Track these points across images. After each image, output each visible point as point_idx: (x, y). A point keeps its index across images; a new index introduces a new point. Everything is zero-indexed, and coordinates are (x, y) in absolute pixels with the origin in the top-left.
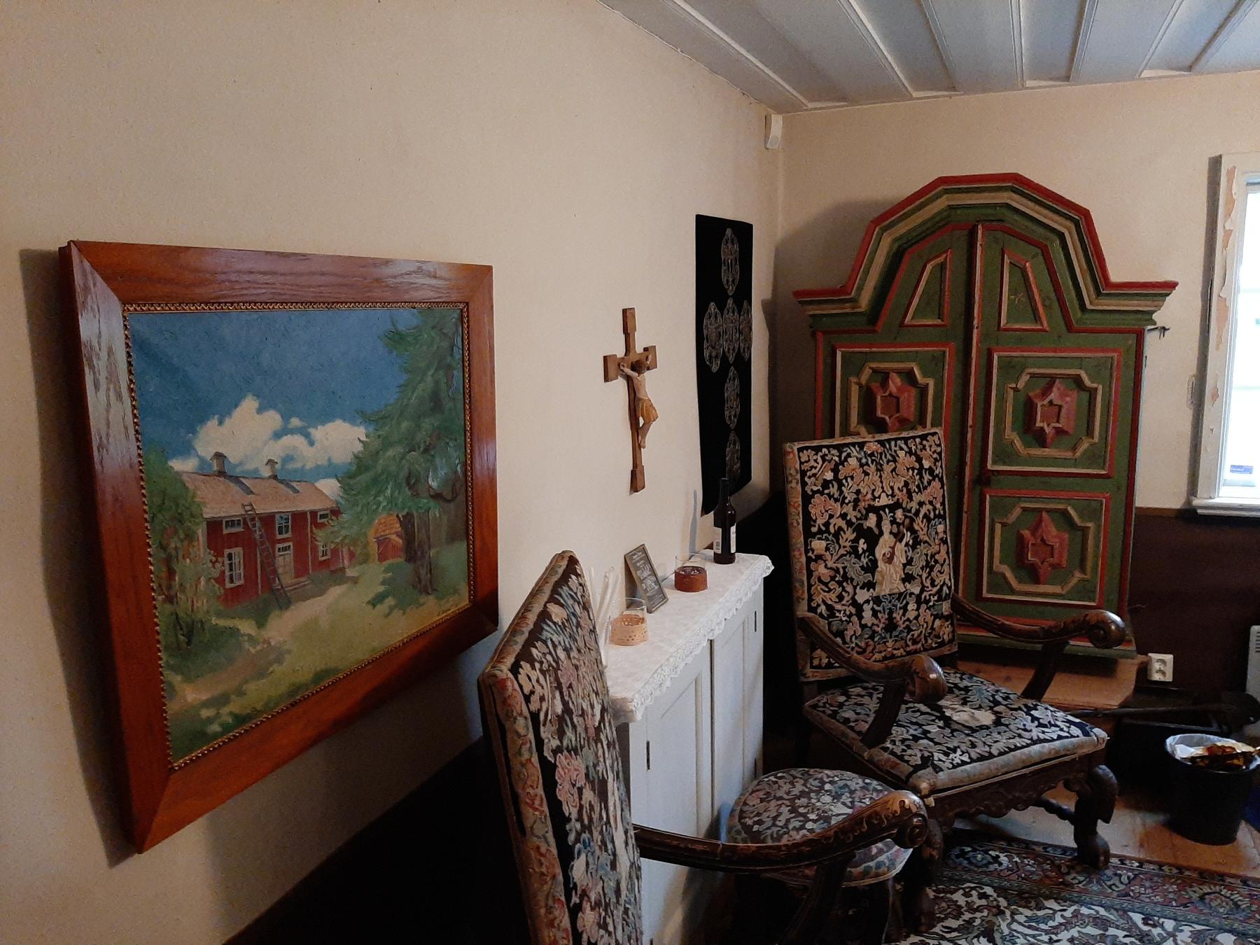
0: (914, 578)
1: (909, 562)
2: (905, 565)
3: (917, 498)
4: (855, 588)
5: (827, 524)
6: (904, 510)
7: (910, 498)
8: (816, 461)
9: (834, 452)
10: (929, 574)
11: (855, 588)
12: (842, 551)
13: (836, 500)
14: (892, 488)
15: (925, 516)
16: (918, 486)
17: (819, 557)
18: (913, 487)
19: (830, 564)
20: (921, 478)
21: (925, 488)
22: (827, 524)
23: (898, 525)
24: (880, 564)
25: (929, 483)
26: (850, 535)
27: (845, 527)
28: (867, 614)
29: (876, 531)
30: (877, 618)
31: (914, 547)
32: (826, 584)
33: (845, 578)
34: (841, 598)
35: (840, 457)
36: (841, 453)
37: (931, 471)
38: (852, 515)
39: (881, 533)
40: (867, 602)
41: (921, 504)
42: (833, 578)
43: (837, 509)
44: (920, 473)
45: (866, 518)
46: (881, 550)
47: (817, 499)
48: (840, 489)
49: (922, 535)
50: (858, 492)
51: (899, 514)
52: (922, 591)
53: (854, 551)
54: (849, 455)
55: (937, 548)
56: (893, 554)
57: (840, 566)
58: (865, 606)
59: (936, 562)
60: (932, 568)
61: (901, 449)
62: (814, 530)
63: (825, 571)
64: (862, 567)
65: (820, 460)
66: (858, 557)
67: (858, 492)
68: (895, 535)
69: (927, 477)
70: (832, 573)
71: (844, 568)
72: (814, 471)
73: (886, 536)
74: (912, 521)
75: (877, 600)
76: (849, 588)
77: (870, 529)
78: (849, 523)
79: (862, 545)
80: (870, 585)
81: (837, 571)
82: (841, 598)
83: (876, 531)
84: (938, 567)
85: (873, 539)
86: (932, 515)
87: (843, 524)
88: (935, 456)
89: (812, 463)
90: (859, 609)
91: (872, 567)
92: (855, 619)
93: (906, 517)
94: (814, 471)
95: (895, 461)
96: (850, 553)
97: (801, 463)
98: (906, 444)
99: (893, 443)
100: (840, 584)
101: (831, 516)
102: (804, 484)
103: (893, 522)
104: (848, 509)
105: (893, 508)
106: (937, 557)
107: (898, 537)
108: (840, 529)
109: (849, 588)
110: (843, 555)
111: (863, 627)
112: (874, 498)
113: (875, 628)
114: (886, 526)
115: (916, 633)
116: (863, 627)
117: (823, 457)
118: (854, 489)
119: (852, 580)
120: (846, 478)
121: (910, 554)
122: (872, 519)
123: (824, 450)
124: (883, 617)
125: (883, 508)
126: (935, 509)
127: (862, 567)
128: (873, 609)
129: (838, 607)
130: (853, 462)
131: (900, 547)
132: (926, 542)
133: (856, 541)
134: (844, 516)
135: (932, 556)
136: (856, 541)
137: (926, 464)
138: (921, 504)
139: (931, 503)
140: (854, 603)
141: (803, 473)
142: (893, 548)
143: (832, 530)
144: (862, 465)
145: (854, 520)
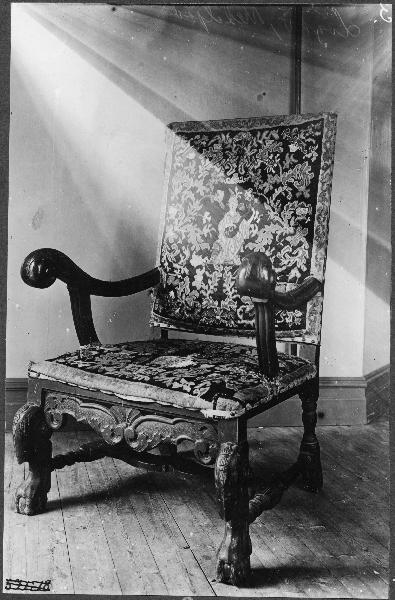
1: (252, 240)
2: (246, 241)
3: (272, 180)
4: (191, 253)
6: (254, 190)
7: (264, 178)
10: (275, 253)
11: (191, 253)
14: (246, 169)
15: (280, 196)
16: (277, 169)
17: (172, 221)
19: (176, 229)
20: (282, 158)
21: (286, 170)
23: (246, 202)
24: (221, 236)
25: (292, 166)
26: (197, 206)
27: (193, 198)
28: (199, 278)
29: (222, 206)
30: (206, 283)
31: (261, 226)
32: (170, 245)
35: (208, 142)
36: (210, 139)
37: (298, 155)
38: (201, 189)
39: (227, 209)
40: (200, 267)
41: (276, 186)
42: (176, 241)
44: (282, 158)
45: (215, 192)
46: (227, 222)
47: (179, 173)
54: (217, 142)
57: (183, 231)
58: (198, 271)
60: (279, 249)
61: (272, 138)
64: (203, 236)
71: (187, 234)
72: (181, 151)
73: (232, 212)
77: (217, 203)
78: (198, 196)
79: (207, 217)
80: (205, 253)
82: (178, 259)
83: (222, 206)
84: (288, 249)
85: (218, 213)
87: (192, 196)
88: (309, 140)
90: (192, 271)
92: (187, 279)
94: (181, 151)
96: (194, 222)
98: (279, 134)
99: (264, 134)
103: (241, 200)
104: (199, 185)
106: (288, 239)
107: (246, 214)
109: (187, 253)
111: (192, 288)
113: (204, 293)
114: (233, 202)
115: (248, 309)
119: (191, 245)
121: (255, 232)
122: (221, 194)
123: (198, 137)
124: (213, 284)
126: (295, 191)
127: (203, 236)
128: (204, 275)
129: (175, 265)
131: (247, 224)
132: (277, 222)
133: (202, 212)
134: (194, 189)
135: (281, 237)
136: (202, 212)
137: (293, 148)
139: (290, 185)
140: (189, 265)
142: (238, 224)
144: (224, 151)
145: (202, 194)
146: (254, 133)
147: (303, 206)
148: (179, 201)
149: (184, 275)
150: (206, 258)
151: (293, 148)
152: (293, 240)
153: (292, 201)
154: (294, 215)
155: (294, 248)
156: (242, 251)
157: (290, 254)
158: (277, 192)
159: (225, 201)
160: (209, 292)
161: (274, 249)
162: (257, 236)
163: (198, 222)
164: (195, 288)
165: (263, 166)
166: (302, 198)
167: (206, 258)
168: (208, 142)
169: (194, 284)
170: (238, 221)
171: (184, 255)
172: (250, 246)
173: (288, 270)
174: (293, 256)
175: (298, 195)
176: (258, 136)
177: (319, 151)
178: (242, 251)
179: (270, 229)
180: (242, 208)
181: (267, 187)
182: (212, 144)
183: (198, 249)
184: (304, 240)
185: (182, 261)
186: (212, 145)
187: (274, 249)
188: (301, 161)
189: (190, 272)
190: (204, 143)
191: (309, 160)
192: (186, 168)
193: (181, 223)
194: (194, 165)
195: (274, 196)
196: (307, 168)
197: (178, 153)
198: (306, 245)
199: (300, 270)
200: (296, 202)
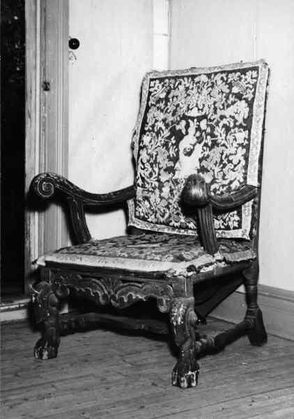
0: (208, 171)
2: (201, 160)
3: (220, 113)
4: (160, 169)
5: (153, 126)
7: (215, 112)
8: (158, 87)
9: (172, 81)
12: (159, 144)
13: (162, 111)
17: (145, 146)
18: (219, 105)
19: (149, 151)
20: (227, 98)
22: (153, 126)
25: (233, 103)
26: (166, 133)
27: (164, 128)
28: (166, 190)
31: (211, 148)
33: (155, 161)
34: (151, 174)
36: (176, 81)
39: (187, 133)
40: (168, 181)
41: (222, 117)
42: (148, 161)
43: (161, 116)
48: (166, 105)
49: (220, 140)
50: (178, 106)
51: (203, 124)
52: (214, 181)
53: (166, 145)
54: (180, 84)
55: (233, 150)
56: (192, 151)
59: (230, 162)
60: (225, 165)
62: (146, 129)
63: (146, 155)
65: (161, 86)
66: (168, 149)
67: (178, 106)
68: (197, 138)
69: (232, 99)
70: (148, 157)
74: (213, 128)
75: (176, 182)
76: (156, 170)
78: (167, 126)
80: (171, 170)
81: (151, 156)
83: (184, 132)
84: (230, 166)
85: (179, 136)
86: (232, 125)
89: (156, 88)
91: (176, 159)
92: (157, 191)
93: (208, 125)
95: (212, 87)
96: (163, 145)
97: (150, 87)
100: (152, 165)
101: (156, 121)
102: (148, 100)
103: (198, 129)
105: (200, 119)
106: (230, 158)
108: (160, 128)
109: (156, 170)
110: (159, 146)
111: (161, 198)
112: (188, 109)
113: (170, 201)
114: (192, 130)
116: (161, 198)
117: (163, 86)
118: (178, 102)
119: (159, 163)
120: (173, 98)
121: (206, 153)
125: (192, 119)
126: (236, 121)
127: (169, 157)
130: (181, 88)
131: (199, 147)
133: (169, 138)
138: (222, 117)
140: (159, 181)
141: (150, 93)
143: (156, 130)
146: (209, 76)
147: (240, 132)
148: (153, 131)
149: (154, 188)
150: (172, 174)
151: (235, 90)
152: (235, 159)
153: (234, 128)
154: (235, 139)
155: (235, 166)
156: (199, 168)
157: (233, 170)
158: (225, 121)
159: (187, 126)
160: (175, 200)
161: (222, 165)
162: (208, 156)
163: (166, 145)
164: (164, 198)
165: (215, 103)
166: (241, 126)
167: (172, 174)
168: (174, 85)
169: (162, 195)
170: (193, 143)
171: (154, 171)
172: (204, 163)
173: (231, 182)
174: (234, 171)
175: (238, 124)
176: (212, 77)
177: (254, 93)
178: (199, 168)
179: (217, 150)
180: (198, 134)
181: (217, 117)
182: (177, 87)
183: (165, 167)
184: (242, 159)
185: (154, 176)
186: (177, 87)
187: (222, 165)
188: (241, 100)
189: (159, 186)
190: (172, 86)
191: (246, 100)
192: (158, 105)
193: (154, 147)
194: (164, 102)
195: (221, 125)
196: (243, 104)
197: (152, 94)
198: (243, 162)
199: (239, 181)
200: (236, 129)
